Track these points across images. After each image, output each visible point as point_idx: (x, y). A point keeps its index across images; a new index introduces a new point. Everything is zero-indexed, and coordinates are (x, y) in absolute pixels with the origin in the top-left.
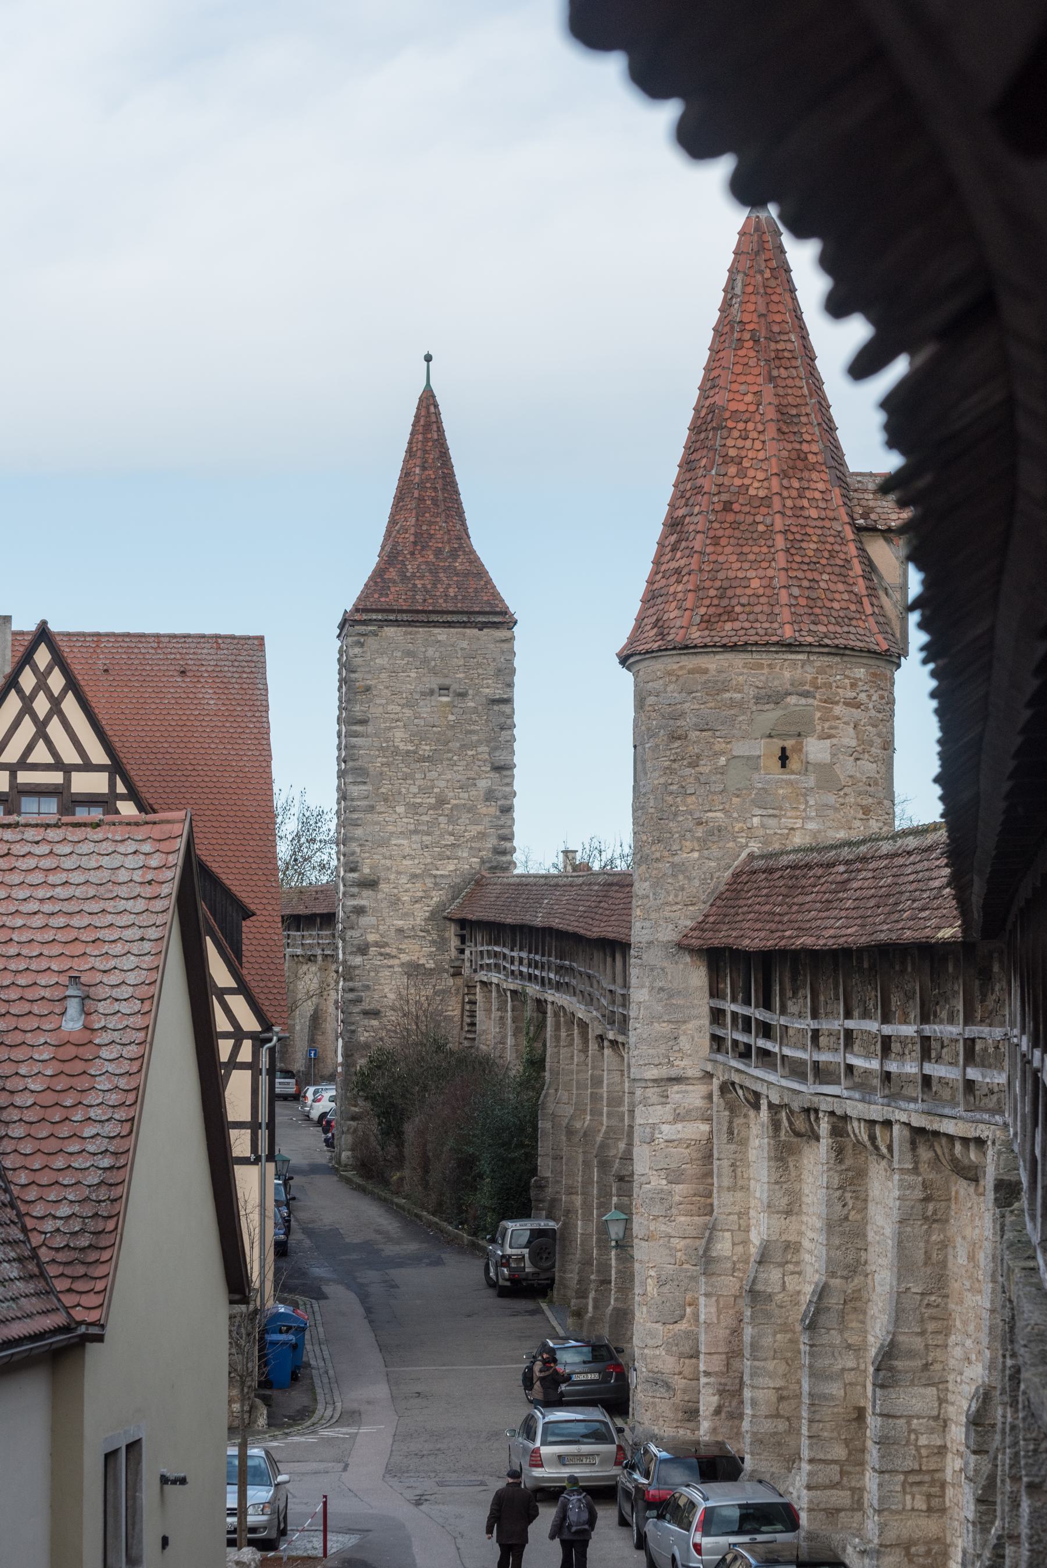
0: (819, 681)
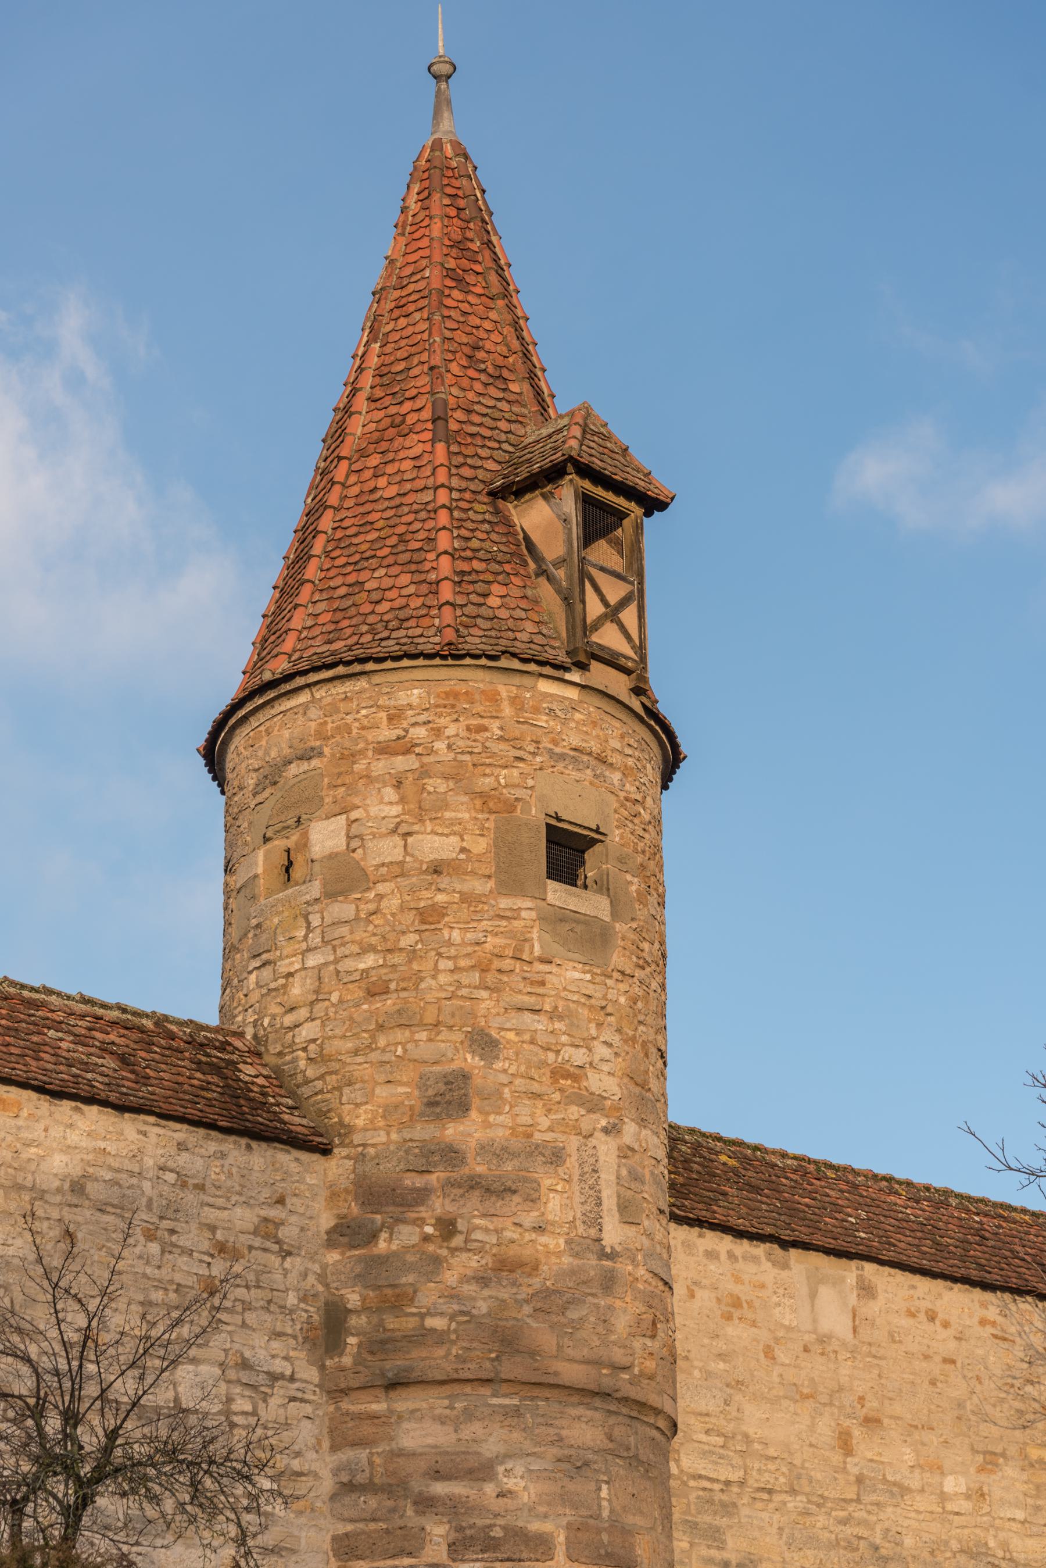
0: (330, 726)
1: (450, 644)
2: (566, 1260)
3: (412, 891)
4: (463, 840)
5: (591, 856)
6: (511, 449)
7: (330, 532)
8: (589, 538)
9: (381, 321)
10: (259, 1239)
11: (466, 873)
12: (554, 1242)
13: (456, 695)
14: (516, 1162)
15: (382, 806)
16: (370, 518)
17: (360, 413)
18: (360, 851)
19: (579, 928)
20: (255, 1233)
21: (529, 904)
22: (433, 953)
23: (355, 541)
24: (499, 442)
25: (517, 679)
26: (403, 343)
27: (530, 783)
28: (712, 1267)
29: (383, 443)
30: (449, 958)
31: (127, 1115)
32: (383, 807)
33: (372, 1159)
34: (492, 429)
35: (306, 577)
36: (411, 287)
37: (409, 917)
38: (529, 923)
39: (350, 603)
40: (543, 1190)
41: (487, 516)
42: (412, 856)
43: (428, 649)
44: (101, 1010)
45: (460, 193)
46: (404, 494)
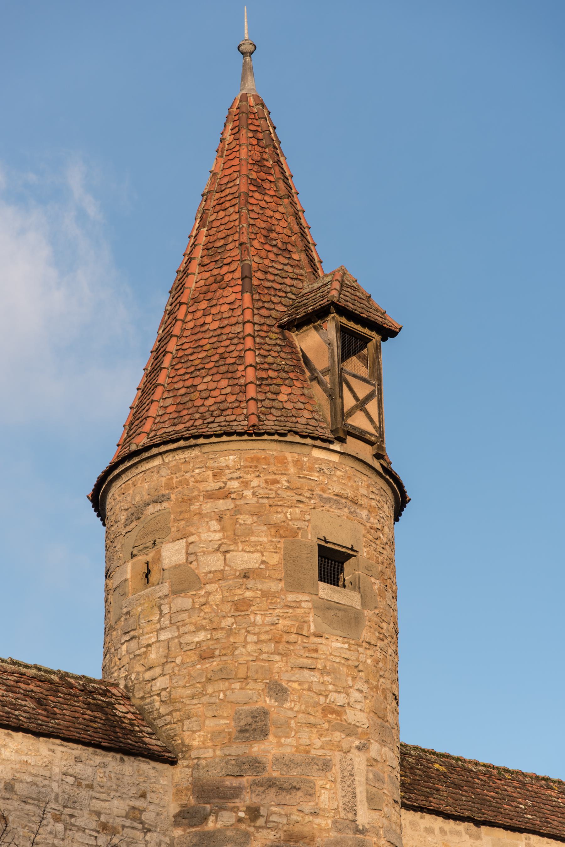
0: (175, 480)
1: (254, 426)
2: (333, 834)
3: (230, 589)
4: (263, 555)
5: (347, 566)
6: (293, 297)
7: (174, 352)
8: (345, 356)
9: (207, 213)
10: (129, 821)
11: (265, 578)
12: (325, 822)
13: (258, 460)
14: (299, 770)
15: (209, 534)
16: (201, 343)
17: (194, 274)
18: (195, 563)
19: (340, 614)
20: (127, 816)
21: (307, 598)
22: (244, 631)
23: (191, 358)
24: (286, 292)
25: (298, 449)
26: (222, 228)
27: (307, 517)
28: (430, 839)
29: (209, 293)
30: (254, 634)
31: (41, 739)
32: (210, 534)
33: (204, 768)
34: (281, 284)
35: (158, 382)
36: (227, 191)
37: (227, 607)
38: (307, 611)
39: (188, 399)
40: (317, 788)
41: (278, 342)
42: (230, 566)
43: (240, 429)
44: (24, 669)
45: (259, 129)
46: (223, 327)
